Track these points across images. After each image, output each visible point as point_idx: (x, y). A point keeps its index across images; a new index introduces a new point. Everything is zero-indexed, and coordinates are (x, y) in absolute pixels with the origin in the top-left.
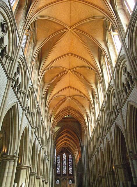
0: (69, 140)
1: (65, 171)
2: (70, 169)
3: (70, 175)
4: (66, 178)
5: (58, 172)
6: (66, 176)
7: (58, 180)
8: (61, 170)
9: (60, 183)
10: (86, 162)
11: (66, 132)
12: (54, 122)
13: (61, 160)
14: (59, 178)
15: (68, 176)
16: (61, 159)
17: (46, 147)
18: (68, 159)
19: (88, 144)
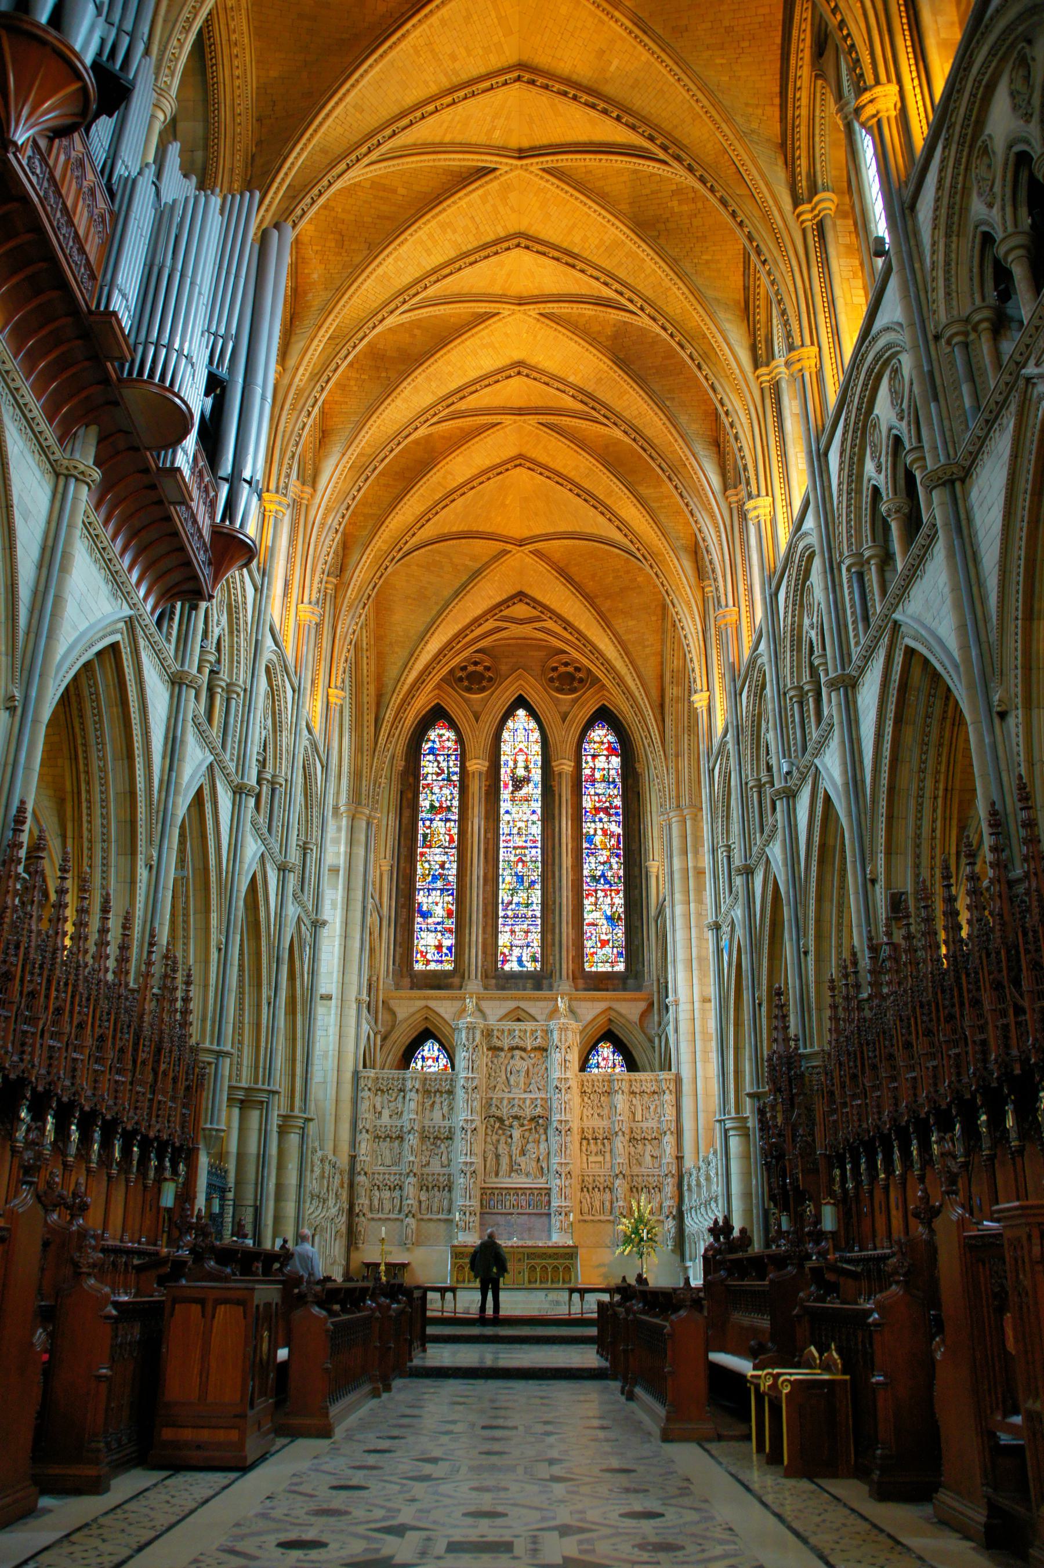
1: (535, 938)
3: (601, 982)
6: (538, 987)
7: (430, 1049)
13: (476, 788)
14: (444, 1007)
15: (565, 986)
16: (477, 765)
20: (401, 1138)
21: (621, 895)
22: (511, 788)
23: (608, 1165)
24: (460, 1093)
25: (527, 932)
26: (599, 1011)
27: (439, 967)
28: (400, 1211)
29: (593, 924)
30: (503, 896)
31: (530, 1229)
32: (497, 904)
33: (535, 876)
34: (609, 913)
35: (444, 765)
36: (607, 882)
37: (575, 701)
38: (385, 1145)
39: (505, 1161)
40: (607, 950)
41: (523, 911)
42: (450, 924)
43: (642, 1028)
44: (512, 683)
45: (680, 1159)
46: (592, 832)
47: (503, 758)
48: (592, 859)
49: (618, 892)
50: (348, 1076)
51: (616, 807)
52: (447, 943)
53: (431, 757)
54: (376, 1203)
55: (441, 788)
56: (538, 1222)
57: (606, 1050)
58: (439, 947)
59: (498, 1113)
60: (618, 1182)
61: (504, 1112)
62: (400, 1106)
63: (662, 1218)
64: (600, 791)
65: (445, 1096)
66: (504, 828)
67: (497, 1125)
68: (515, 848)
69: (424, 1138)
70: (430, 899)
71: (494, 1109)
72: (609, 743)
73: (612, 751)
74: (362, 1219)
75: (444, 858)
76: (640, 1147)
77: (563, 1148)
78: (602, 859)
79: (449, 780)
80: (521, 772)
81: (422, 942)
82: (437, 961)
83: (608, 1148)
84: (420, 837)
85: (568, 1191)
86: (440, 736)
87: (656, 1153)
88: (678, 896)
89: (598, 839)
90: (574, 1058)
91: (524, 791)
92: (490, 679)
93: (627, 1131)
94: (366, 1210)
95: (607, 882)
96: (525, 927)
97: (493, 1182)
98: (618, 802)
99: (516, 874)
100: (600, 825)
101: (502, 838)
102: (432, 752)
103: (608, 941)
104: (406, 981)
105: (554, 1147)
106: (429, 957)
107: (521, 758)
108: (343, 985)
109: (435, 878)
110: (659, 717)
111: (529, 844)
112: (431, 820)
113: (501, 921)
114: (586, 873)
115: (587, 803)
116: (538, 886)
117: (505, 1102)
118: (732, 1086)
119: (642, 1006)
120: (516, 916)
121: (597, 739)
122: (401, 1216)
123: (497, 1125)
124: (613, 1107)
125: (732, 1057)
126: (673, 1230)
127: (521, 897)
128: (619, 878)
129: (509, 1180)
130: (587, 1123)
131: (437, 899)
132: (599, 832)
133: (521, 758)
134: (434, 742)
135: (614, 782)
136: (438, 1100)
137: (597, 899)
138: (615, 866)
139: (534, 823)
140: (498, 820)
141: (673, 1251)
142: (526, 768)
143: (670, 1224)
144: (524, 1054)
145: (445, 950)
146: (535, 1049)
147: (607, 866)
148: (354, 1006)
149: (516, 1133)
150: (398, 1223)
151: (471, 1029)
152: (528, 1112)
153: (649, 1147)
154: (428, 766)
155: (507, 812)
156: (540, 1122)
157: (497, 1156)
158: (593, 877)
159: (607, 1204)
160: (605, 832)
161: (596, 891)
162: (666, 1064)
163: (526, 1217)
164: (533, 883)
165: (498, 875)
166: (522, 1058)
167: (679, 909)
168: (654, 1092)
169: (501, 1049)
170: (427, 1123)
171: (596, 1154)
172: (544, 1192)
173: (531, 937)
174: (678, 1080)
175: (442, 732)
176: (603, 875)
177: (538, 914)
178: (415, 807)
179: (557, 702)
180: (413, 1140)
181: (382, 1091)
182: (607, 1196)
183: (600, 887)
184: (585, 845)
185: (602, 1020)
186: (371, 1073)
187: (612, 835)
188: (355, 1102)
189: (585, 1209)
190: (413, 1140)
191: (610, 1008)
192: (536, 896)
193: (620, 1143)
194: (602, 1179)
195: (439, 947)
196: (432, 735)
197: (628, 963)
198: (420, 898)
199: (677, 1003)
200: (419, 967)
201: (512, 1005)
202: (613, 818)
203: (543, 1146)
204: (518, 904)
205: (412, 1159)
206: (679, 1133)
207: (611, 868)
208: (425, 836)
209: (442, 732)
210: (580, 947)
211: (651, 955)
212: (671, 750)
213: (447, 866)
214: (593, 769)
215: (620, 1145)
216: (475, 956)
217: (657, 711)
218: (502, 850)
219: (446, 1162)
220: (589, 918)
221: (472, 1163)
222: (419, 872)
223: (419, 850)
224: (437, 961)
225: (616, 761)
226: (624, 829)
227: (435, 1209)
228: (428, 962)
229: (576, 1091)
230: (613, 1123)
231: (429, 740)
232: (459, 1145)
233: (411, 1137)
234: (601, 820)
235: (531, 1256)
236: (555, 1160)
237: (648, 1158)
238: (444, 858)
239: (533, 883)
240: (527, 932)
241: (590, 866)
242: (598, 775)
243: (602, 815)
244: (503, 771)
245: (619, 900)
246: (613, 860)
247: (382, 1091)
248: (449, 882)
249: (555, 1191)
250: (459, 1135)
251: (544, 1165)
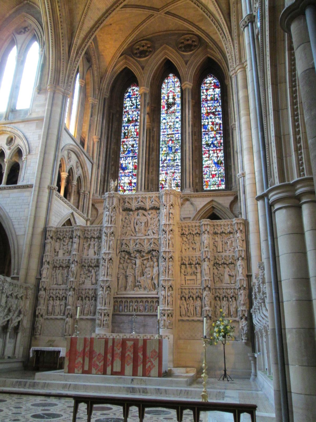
20: (68, 267)
21: (222, 152)
22: (166, 108)
23: (199, 282)
24: (104, 237)
25: (174, 173)
26: (207, 202)
27: (130, 193)
28: (64, 314)
29: (207, 167)
30: (162, 157)
31: (144, 326)
32: (159, 161)
33: (178, 147)
34: (216, 161)
35: (134, 102)
36: (214, 146)
37: (192, 55)
38: (58, 271)
39: (130, 279)
40: (215, 179)
43: (232, 211)
44: (161, 52)
45: (249, 277)
46: (206, 124)
47: (162, 96)
48: (207, 136)
49: (220, 150)
51: (218, 111)
52: (134, 181)
53: (128, 99)
54: (50, 308)
55: (133, 112)
56: (150, 321)
58: (130, 183)
59: (127, 249)
60: (205, 293)
61: (132, 247)
62: (69, 247)
63: (237, 319)
64: (210, 105)
65: (96, 240)
66: (162, 126)
67: (127, 257)
68: (168, 135)
70: (127, 162)
71: (124, 246)
72: (214, 83)
73: (216, 86)
74: (40, 319)
75: (134, 142)
76: (221, 269)
77: (167, 270)
78: (212, 136)
79: (137, 108)
80: (171, 100)
81: (122, 182)
82: (129, 190)
83: (199, 270)
84: (123, 134)
85: (170, 299)
86: (133, 90)
87: (233, 273)
88: (242, 112)
89: (209, 127)
91: (172, 109)
92: (150, 52)
93: (212, 258)
94: (43, 312)
95: (214, 146)
96: (173, 171)
98: (219, 109)
99: (169, 147)
100: (210, 120)
101: (162, 131)
102: (129, 96)
103: (216, 174)
105: (162, 269)
106: (125, 188)
107: (171, 95)
108: (41, 179)
109: (129, 152)
110: (228, 19)
111: (176, 132)
112: (128, 126)
113: (161, 169)
114: (203, 143)
115: (204, 111)
116: (179, 151)
117: (132, 242)
118: (275, 160)
119: (232, 198)
120: (168, 166)
121: (208, 82)
122: (64, 317)
123: (127, 257)
124: (202, 243)
125: (272, 123)
126: (245, 328)
128: (221, 144)
129: (133, 292)
130: (184, 253)
131: (130, 161)
132: (210, 123)
133: (171, 95)
134: (130, 92)
135: (217, 100)
136: (92, 243)
137: (209, 154)
138: (219, 138)
139: (177, 122)
141: (246, 344)
142: (174, 99)
143: (243, 323)
144: (146, 213)
145: (133, 184)
146: (153, 208)
147: (214, 139)
148: (47, 191)
149: (138, 262)
150: (62, 322)
152: (147, 247)
153: (227, 269)
155: (164, 119)
157: (126, 277)
158: (208, 145)
159: (198, 308)
160: (213, 124)
161: (209, 151)
163: (142, 318)
164: (177, 149)
165: (159, 148)
166: (144, 215)
167: (243, 120)
168: (230, 233)
169: (130, 210)
170: (85, 256)
171: (191, 275)
172: (155, 300)
173: (176, 175)
174: (246, 223)
175: (133, 88)
176: (212, 143)
177: (180, 164)
178: (120, 121)
179: (183, 56)
181: (60, 239)
182: (198, 303)
183: (211, 149)
184: (203, 130)
185: (209, 207)
187: (217, 124)
188: (44, 246)
189: (183, 312)
190: (74, 267)
191: (212, 201)
192: (178, 156)
193: (205, 265)
194: (194, 291)
198: (122, 161)
199: (243, 175)
202: (216, 117)
203: (156, 269)
204: (169, 160)
205: (72, 279)
206: (248, 259)
207: (216, 140)
208: (125, 133)
209: (133, 88)
212: (235, 34)
213: (135, 146)
214: (207, 95)
215: (206, 267)
217: (226, 17)
218: (161, 137)
219: (94, 282)
220: (205, 164)
221: (107, 281)
222: (122, 150)
223: (122, 140)
224: (129, 190)
225: (218, 90)
226: (223, 121)
227: (86, 312)
228: (125, 191)
230: (202, 253)
231: (127, 92)
232: (102, 271)
233: (73, 266)
234: (211, 118)
236: (162, 278)
237: (227, 277)
238: (134, 142)
239: (177, 149)
240: (174, 173)
241: (205, 139)
242: (209, 98)
243: (211, 115)
244: (162, 101)
245: (221, 154)
247: (60, 239)
248: (136, 153)
249: (161, 298)
251: (156, 282)
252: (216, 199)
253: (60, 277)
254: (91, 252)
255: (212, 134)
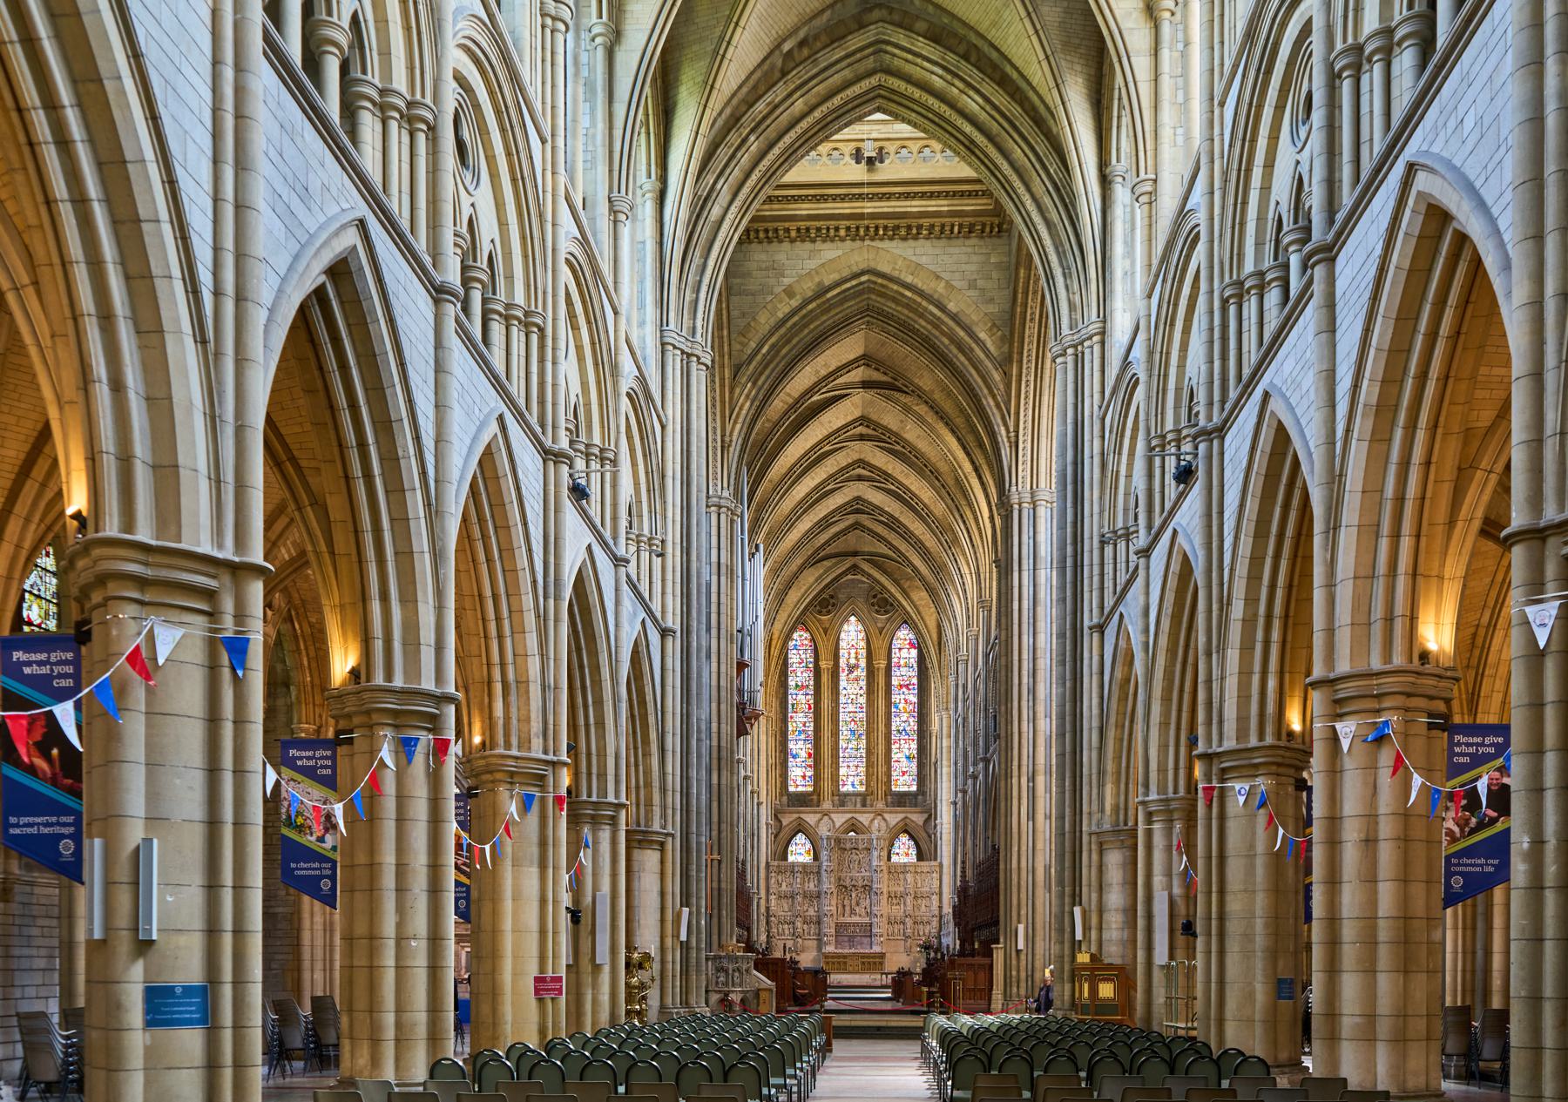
0: (887, 476)
1: (862, 770)
2: (904, 752)
3: (902, 800)
4: (864, 819)
5: (799, 777)
8: (823, 757)
9: (816, 858)
10: (1044, 663)
11: (861, 430)
12: (701, 205)
14: (811, 819)
15: (880, 805)
17: (614, 462)
18: (883, 664)
19: (1092, 447)
20: (792, 897)
30: (842, 744)
37: (888, 619)
38: (784, 902)
39: (847, 908)
40: (906, 777)
41: (854, 753)
42: (811, 762)
45: (940, 907)
50: (763, 865)
56: (866, 940)
57: (904, 838)
58: (804, 777)
61: (848, 883)
66: (842, 699)
69: (805, 897)
73: (912, 645)
78: (904, 719)
80: (853, 661)
88: (945, 762)
89: (901, 706)
90: (884, 854)
91: (855, 673)
97: (842, 920)
98: (915, 681)
104: (785, 799)
107: (853, 651)
114: (893, 728)
115: (895, 681)
119: (926, 816)
124: (905, 880)
127: (853, 744)
130: (893, 889)
140: (838, 694)
151: (828, 838)
152: (860, 883)
154: (794, 658)
156: (867, 888)
162: (935, 859)
173: (860, 769)
174: (941, 865)
179: (875, 621)
180: (799, 898)
185: (901, 824)
186: (776, 863)
188: (767, 879)
190: (799, 898)
192: (863, 743)
193: (909, 899)
195: (804, 777)
196: (795, 635)
197: (919, 785)
198: (791, 745)
200: (792, 789)
201: (849, 816)
206: (941, 894)
210: (889, 776)
211: (930, 786)
216: (826, 786)
220: (895, 757)
225: (914, 652)
229: (885, 871)
235: (863, 957)
242: (902, 662)
245: (914, 746)
246: (911, 720)
250: (823, 896)
252: (909, 815)
253: (785, 905)
254: (812, 885)
255: (904, 717)
